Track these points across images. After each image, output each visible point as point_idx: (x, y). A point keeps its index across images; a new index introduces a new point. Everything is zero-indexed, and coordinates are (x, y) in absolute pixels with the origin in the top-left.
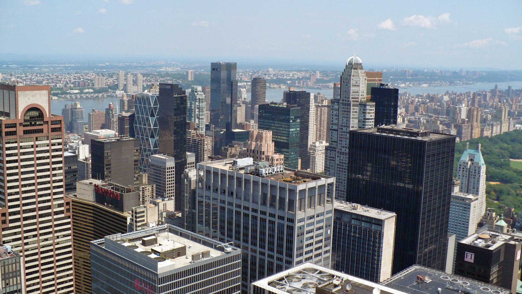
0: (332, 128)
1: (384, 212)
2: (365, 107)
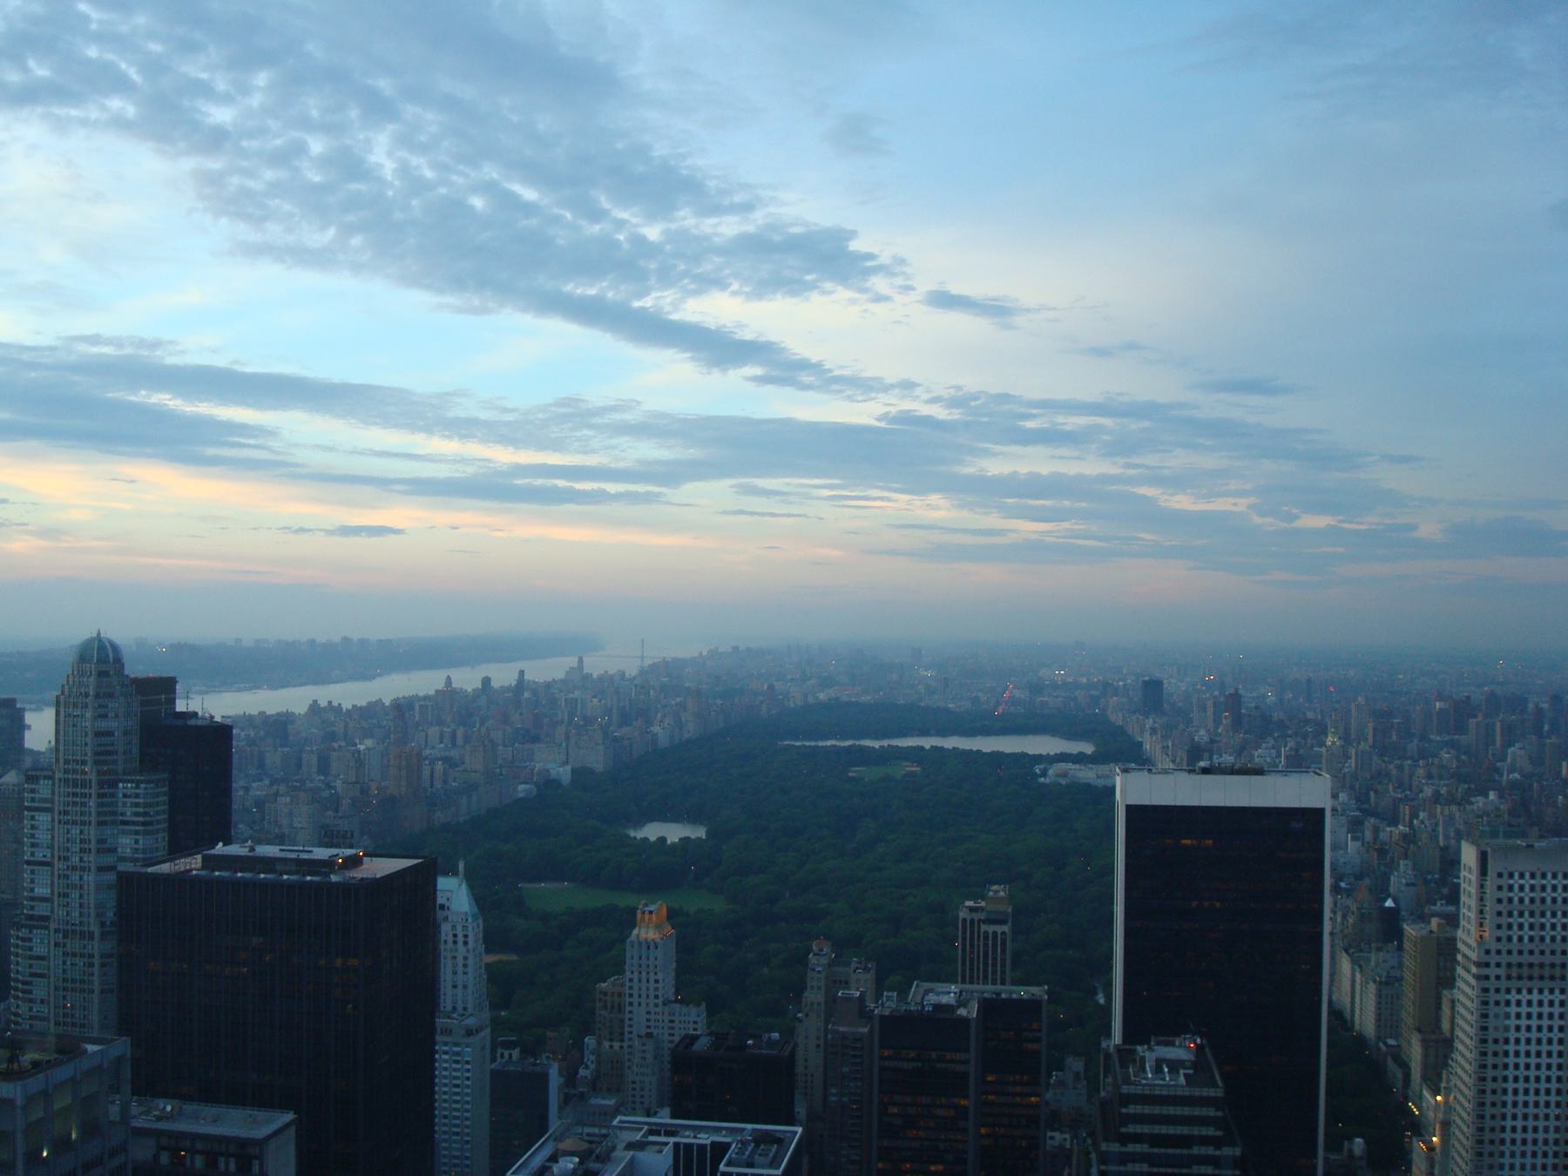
0: (32, 859)
1: (261, 1114)
2: (137, 787)
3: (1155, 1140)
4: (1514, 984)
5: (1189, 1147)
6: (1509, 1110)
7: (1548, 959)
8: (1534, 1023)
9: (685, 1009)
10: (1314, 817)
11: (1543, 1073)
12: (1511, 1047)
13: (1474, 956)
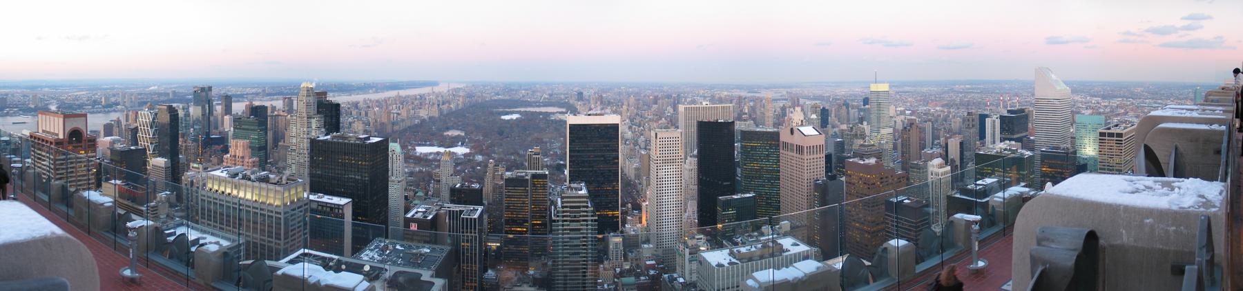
3: (571, 207)
4: (664, 164)
7: (672, 158)
11: (672, 185)
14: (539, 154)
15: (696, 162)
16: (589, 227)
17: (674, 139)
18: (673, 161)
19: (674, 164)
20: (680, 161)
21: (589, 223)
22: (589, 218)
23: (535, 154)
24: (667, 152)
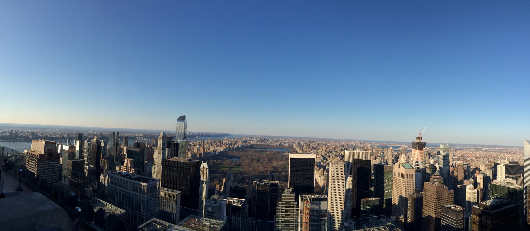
3: (286, 202)
4: (335, 180)
5: (290, 202)
6: (335, 197)
7: (339, 177)
8: (338, 185)
9: (234, 183)
10: (314, 159)
11: (339, 192)
12: (335, 188)
13: (331, 177)
14: (275, 173)
15: (352, 180)
16: (295, 214)
17: (341, 168)
18: (340, 179)
19: (341, 180)
20: (343, 179)
21: (295, 211)
22: (295, 208)
23: (273, 172)
24: (337, 174)
